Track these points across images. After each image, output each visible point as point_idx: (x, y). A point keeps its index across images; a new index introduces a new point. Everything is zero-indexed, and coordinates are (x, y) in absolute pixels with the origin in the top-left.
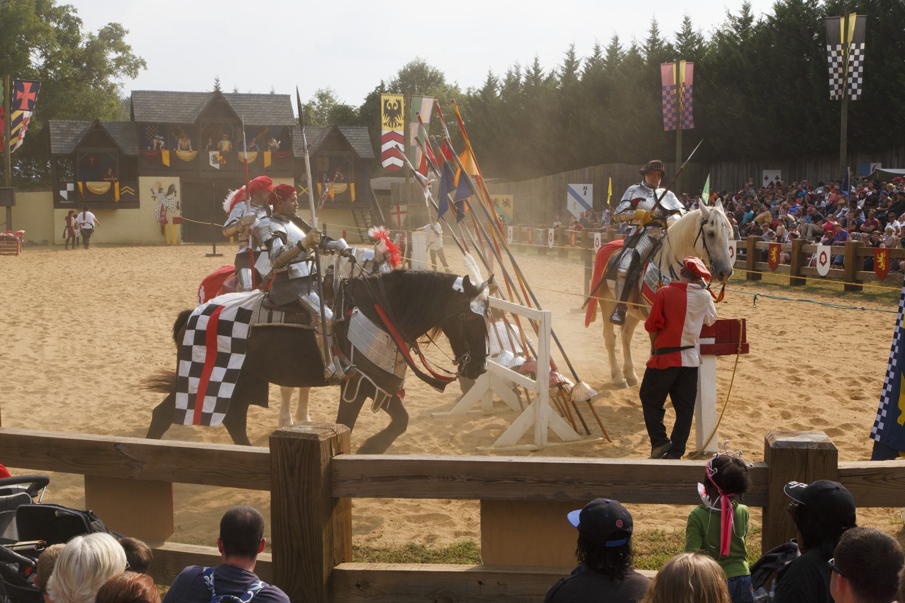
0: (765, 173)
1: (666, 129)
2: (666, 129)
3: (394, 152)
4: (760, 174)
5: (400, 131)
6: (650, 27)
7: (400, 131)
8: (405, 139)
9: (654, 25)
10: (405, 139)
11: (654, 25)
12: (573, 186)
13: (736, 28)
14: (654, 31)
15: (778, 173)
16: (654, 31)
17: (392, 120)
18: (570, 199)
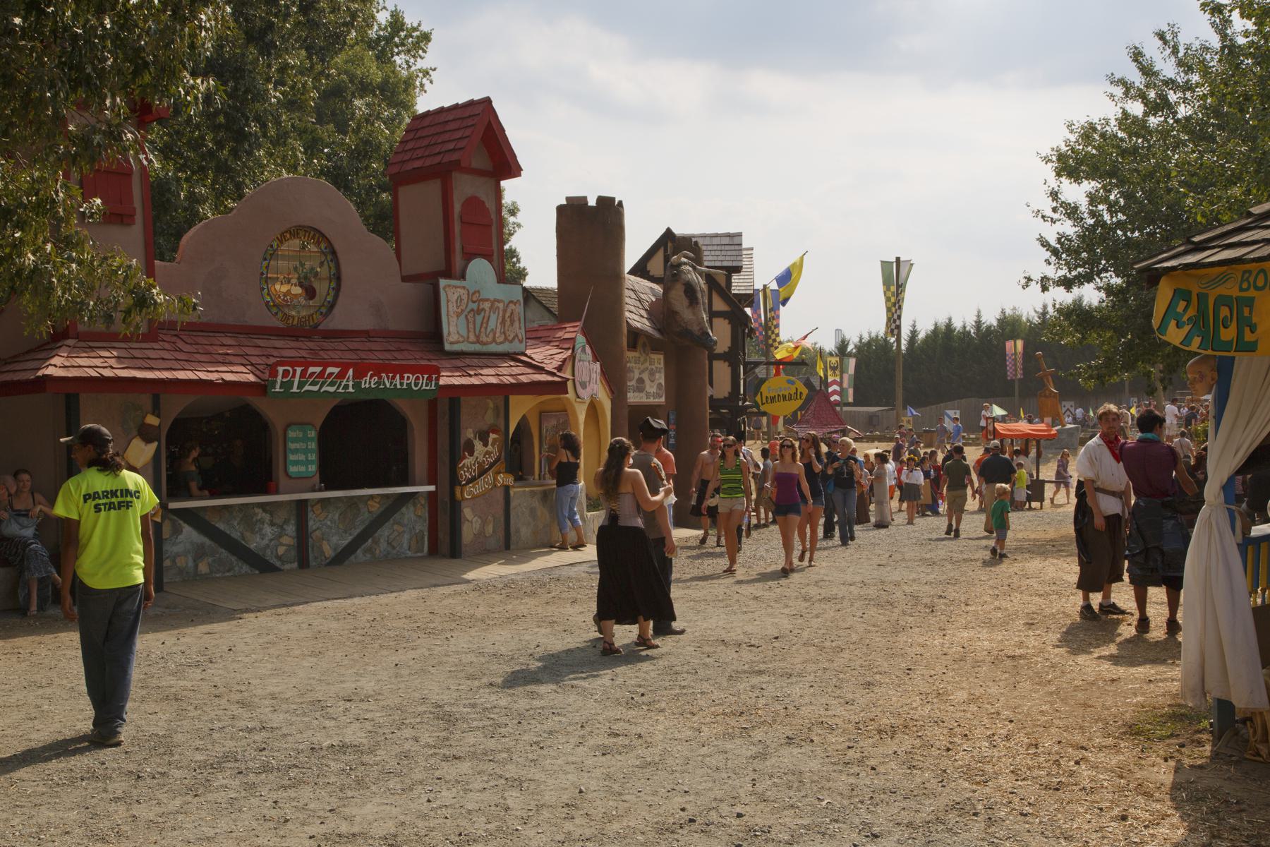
0: (1063, 403)
1: (1009, 378)
2: (1009, 378)
3: (835, 392)
4: (1061, 404)
5: (838, 379)
6: (976, 313)
7: (838, 379)
8: (840, 384)
9: (979, 312)
10: (840, 384)
11: (979, 312)
12: (949, 412)
13: (1039, 318)
14: (979, 316)
15: (1072, 403)
16: (979, 316)
17: (834, 372)
18: (946, 419)
